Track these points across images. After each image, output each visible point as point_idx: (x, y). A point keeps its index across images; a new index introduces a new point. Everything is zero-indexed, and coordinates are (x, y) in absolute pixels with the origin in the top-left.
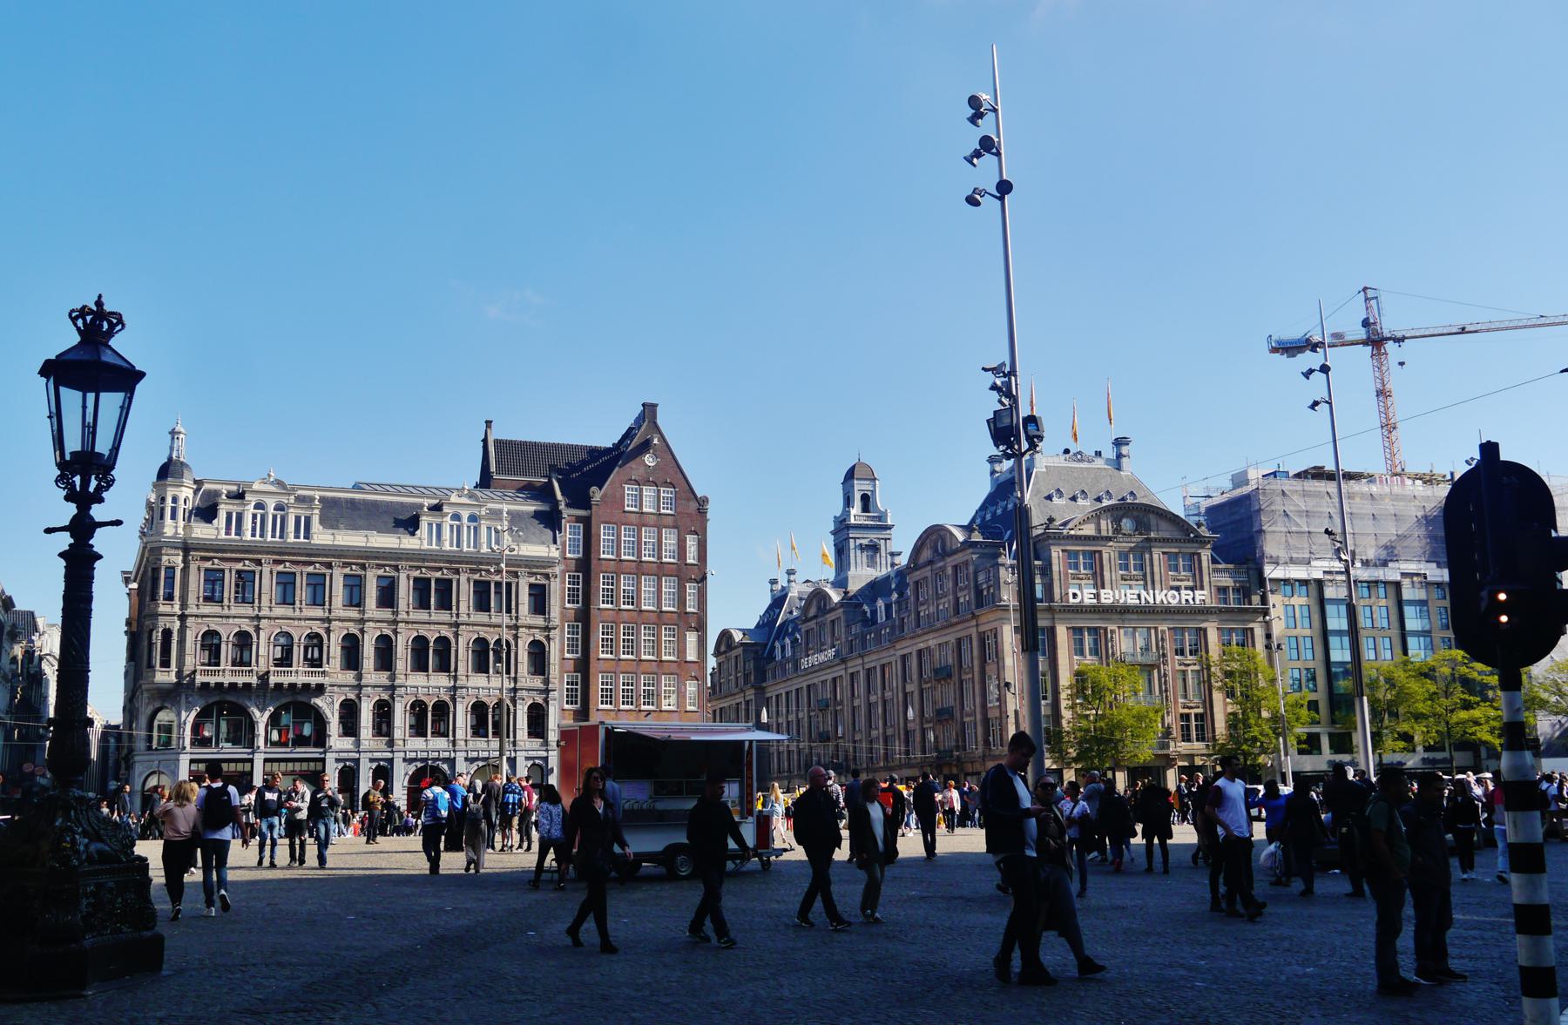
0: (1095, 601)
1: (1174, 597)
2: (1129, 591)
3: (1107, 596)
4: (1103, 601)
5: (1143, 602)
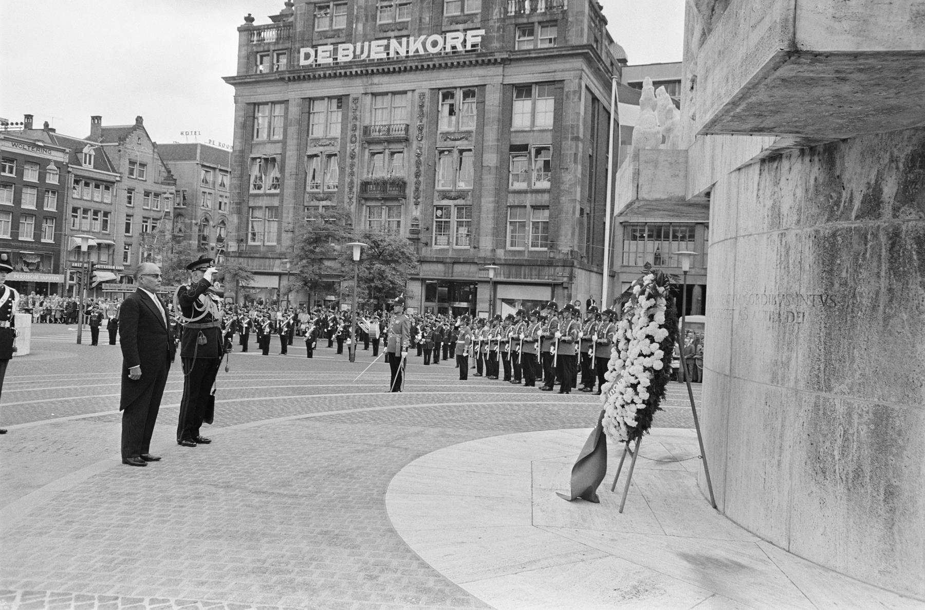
0: (331, 61)
1: (435, 44)
2: (374, 43)
3: (346, 53)
4: (341, 59)
5: (392, 55)
